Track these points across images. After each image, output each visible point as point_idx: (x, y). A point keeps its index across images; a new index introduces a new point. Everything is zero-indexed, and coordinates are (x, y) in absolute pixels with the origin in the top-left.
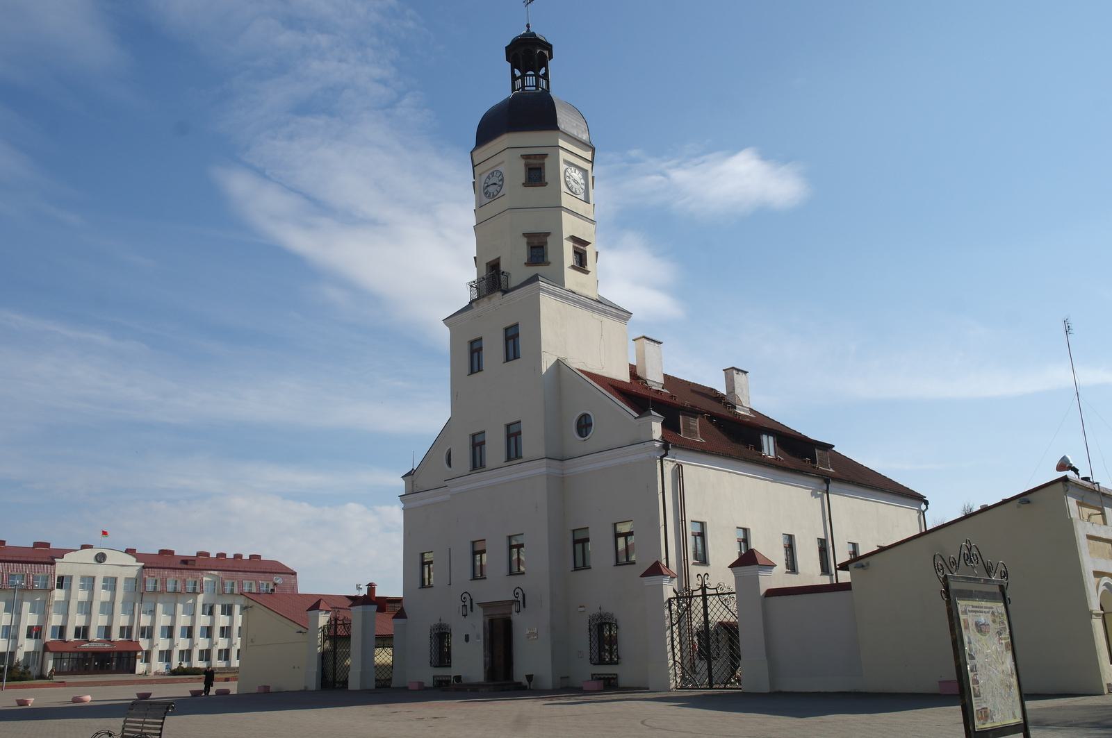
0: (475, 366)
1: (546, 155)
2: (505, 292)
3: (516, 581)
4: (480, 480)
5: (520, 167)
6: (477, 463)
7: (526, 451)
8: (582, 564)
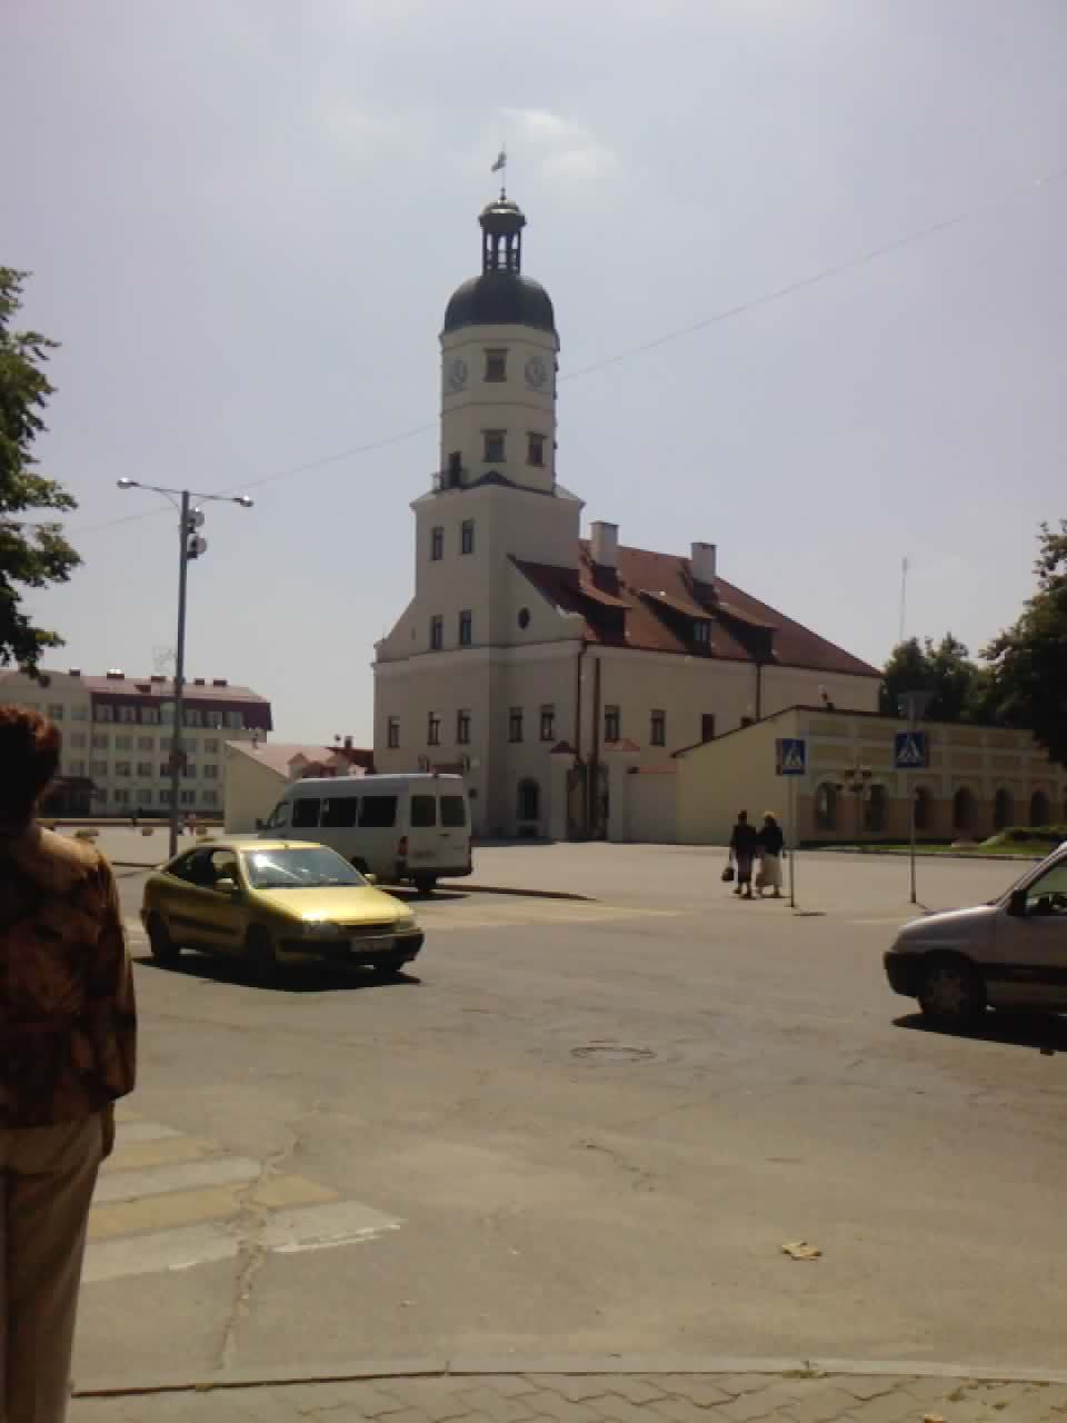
0: (437, 554)
1: (505, 351)
2: (464, 487)
3: (464, 748)
4: (438, 659)
5: (483, 360)
6: (436, 645)
7: (474, 639)
8: (517, 738)
